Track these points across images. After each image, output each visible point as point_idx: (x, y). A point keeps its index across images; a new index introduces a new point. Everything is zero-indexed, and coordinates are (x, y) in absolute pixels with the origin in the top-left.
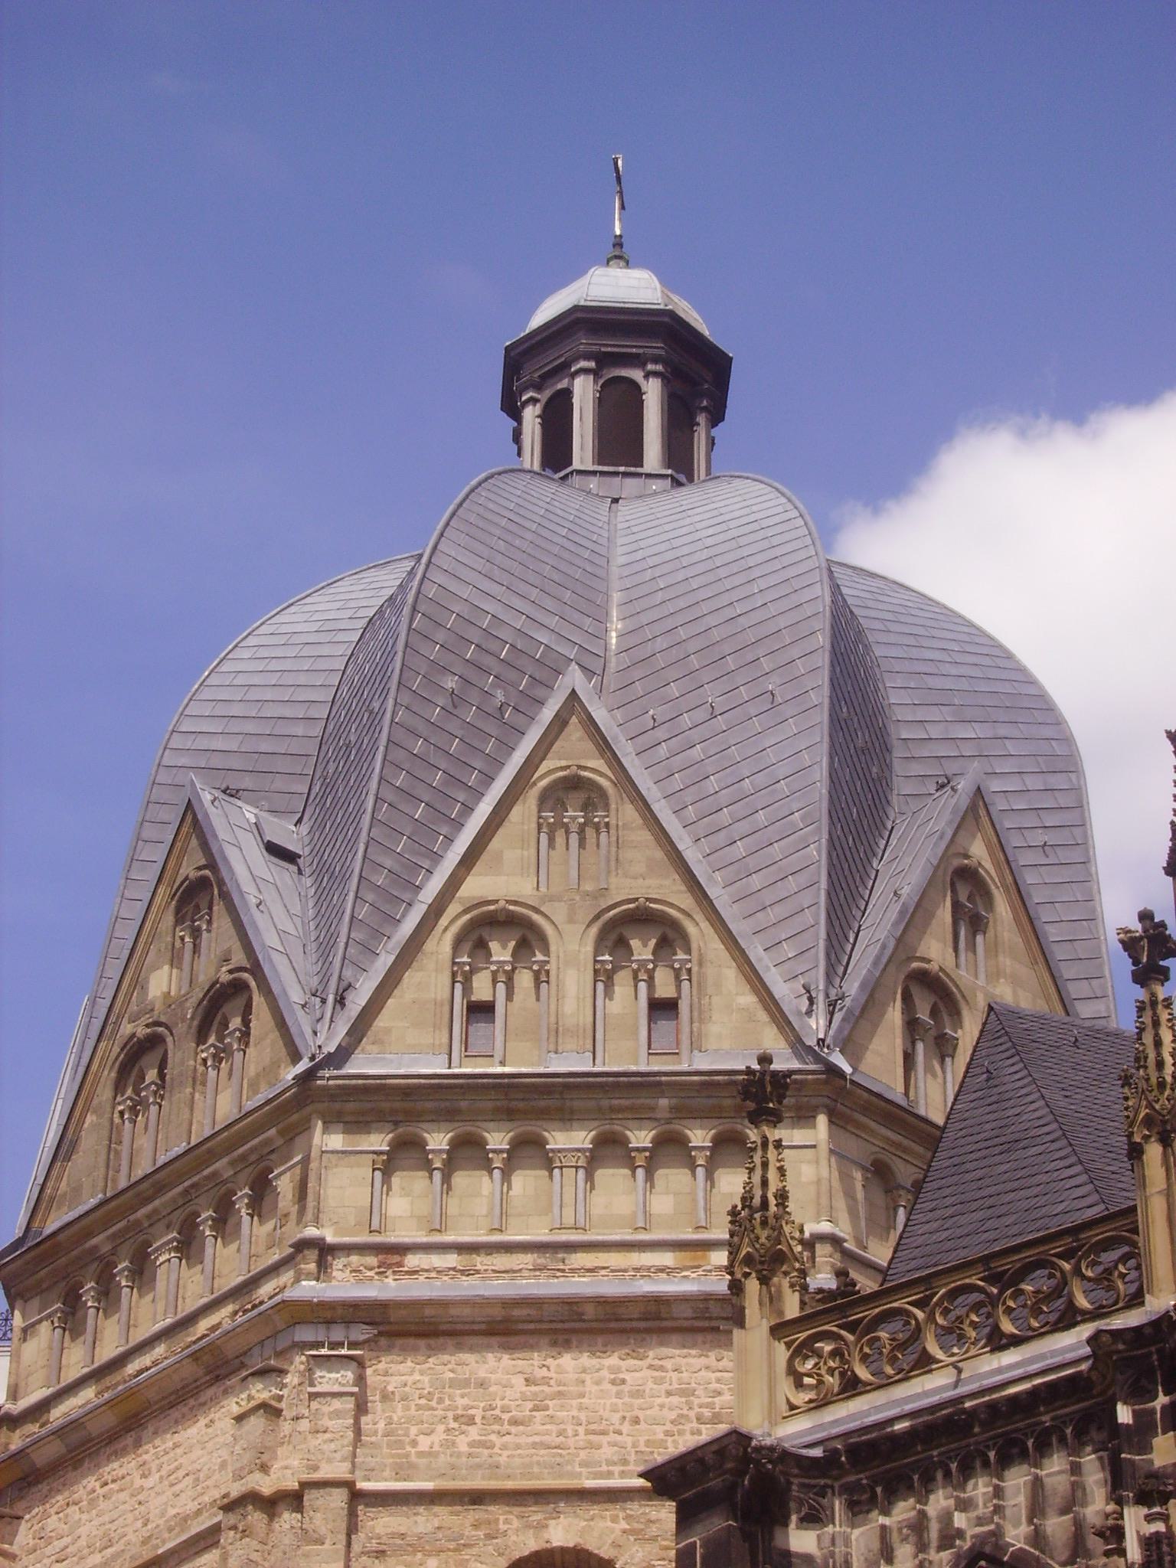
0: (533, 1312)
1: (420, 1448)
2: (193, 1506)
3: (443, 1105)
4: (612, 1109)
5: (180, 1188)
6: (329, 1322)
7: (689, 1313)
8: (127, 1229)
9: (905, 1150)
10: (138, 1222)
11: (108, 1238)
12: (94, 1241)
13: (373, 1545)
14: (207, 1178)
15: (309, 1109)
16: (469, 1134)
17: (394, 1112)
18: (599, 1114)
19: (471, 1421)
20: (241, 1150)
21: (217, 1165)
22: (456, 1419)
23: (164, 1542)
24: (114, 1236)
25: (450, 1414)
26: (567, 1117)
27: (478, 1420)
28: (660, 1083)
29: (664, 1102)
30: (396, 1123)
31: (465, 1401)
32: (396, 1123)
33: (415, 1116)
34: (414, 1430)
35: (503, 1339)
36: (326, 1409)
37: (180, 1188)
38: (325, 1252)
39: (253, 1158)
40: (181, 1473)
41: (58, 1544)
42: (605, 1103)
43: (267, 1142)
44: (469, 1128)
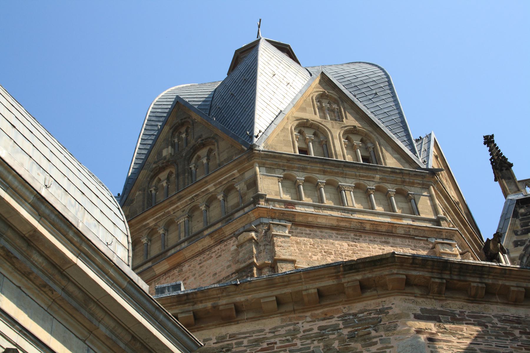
0: (347, 225)
1: (313, 259)
3: (301, 166)
4: (360, 176)
5: (191, 197)
6: (273, 219)
7: (403, 232)
8: (163, 215)
9: (449, 212)
10: (169, 212)
11: (154, 220)
14: (203, 192)
15: (252, 161)
16: (310, 177)
17: (284, 166)
18: (355, 177)
20: (219, 180)
21: (209, 187)
22: (325, 252)
24: (157, 218)
25: (323, 251)
26: (345, 176)
27: (333, 253)
28: (377, 169)
29: (378, 176)
30: (284, 170)
31: (327, 248)
32: (284, 170)
33: (291, 168)
34: (310, 254)
35: (336, 232)
36: (279, 240)
37: (188, 198)
38: (268, 201)
39: (225, 182)
42: (358, 174)
43: (234, 174)
44: (310, 175)
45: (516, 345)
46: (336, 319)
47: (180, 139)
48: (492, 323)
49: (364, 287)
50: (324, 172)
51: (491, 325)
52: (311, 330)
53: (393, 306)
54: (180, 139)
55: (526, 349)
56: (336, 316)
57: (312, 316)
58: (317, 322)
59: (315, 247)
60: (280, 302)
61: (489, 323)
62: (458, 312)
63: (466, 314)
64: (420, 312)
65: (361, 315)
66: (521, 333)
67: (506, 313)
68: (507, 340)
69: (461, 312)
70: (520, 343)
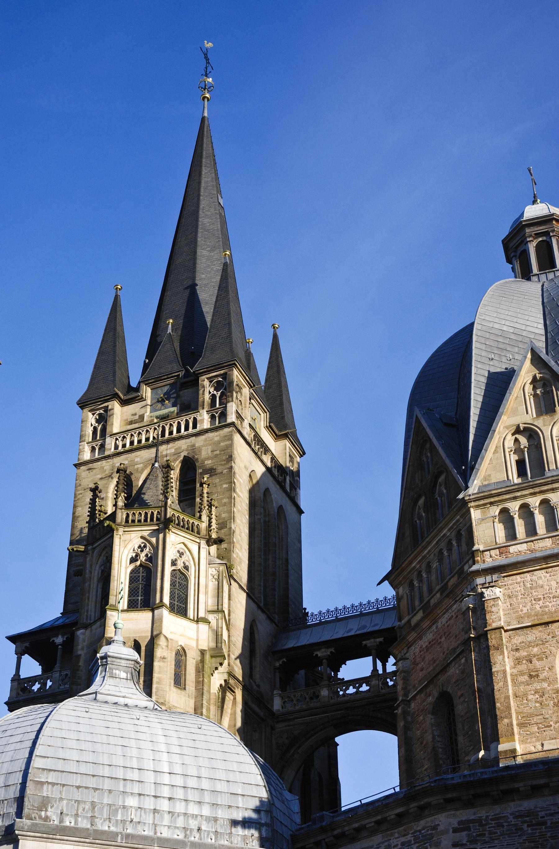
2: (456, 645)
10: (425, 556)
12: (414, 565)
13: (514, 647)
14: (443, 536)
19: (540, 599)
21: (445, 532)
23: (449, 659)
34: (521, 606)
39: (455, 527)
40: (451, 635)
41: (420, 666)
43: (458, 521)
45: (521, 841)
46: (410, 835)
47: (427, 457)
48: (508, 822)
49: (422, 808)
50: (534, 494)
51: (507, 824)
52: (397, 845)
53: (440, 823)
54: (427, 457)
55: (529, 842)
56: (411, 832)
57: (398, 833)
58: (401, 839)
59: (526, 596)
60: (378, 823)
61: (505, 822)
62: (484, 818)
63: (490, 817)
64: (457, 826)
65: (423, 832)
66: (528, 826)
67: (522, 808)
68: (516, 836)
69: (487, 817)
70: (525, 838)
